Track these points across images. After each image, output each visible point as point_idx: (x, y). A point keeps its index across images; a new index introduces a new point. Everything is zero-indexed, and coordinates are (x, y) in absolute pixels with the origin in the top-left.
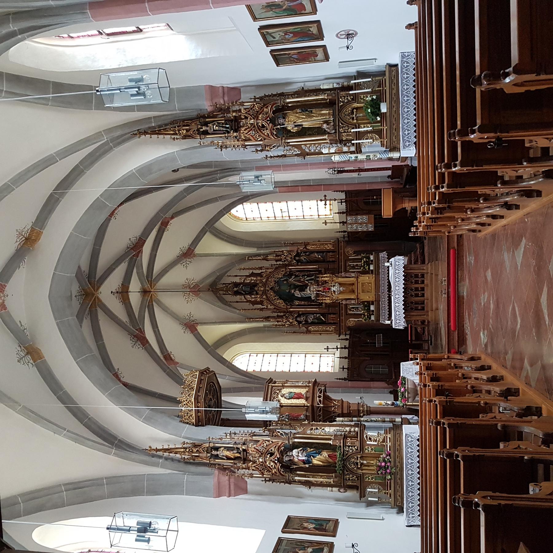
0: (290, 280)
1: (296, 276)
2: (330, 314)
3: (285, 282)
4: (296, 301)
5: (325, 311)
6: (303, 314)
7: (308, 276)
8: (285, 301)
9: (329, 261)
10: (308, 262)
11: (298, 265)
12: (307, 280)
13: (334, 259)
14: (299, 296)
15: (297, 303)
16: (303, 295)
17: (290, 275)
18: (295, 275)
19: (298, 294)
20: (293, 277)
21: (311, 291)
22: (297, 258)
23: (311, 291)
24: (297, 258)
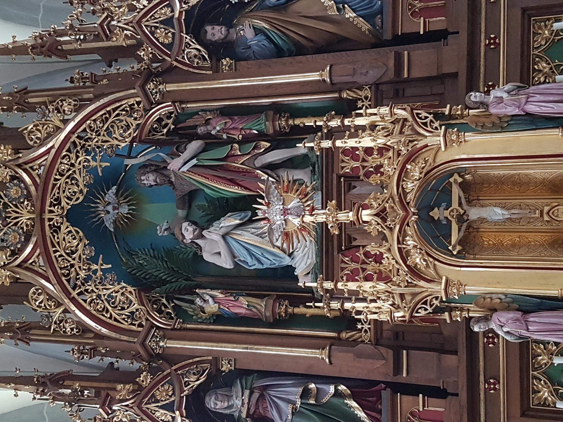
0: (174, 164)
1: (212, 142)
2: (412, 390)
3: (149, 179)
4: (207, 293)
5: (376, 368)
6: (241, 374)
7: (281, 140)
8: (144, 286)
9: (413, 39)
10: (279, 53)
11: (217, 72)
12: (270, 168)
13: (438, 22)
14: (226, 263)
15: (211, 301)
16: (242, 255)
17: (180, 134)
18: (207, 136)
19: (215, 248)
20: (194, 146)
21: (286, 228)
22: (215, 32)
23: (286, 228)
24: (215, 32)
